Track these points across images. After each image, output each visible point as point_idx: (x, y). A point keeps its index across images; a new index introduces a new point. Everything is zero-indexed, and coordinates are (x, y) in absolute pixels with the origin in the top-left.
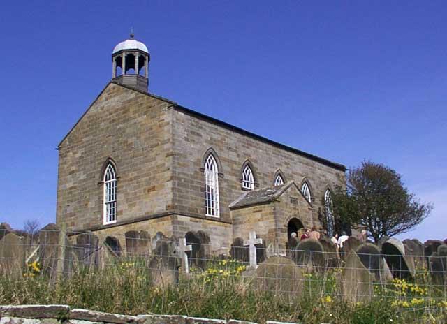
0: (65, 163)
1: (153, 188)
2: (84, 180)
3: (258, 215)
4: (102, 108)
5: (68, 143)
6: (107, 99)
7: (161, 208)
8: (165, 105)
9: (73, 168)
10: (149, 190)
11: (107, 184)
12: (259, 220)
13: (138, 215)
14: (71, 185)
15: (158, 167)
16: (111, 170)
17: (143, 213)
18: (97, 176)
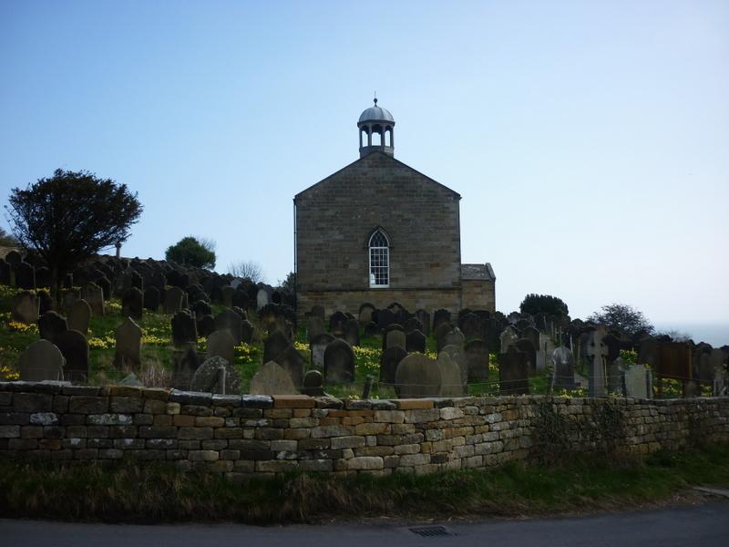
0: (309, 217)
1: (437, 265)
2: (342, 241)
3: (478, 290)
4: (365, 174)
5: (311, 196)
6: (370, 167)
7: (448, 283)
8: (450, 196)
9: (321, 225)
10: (432, 266)
11: (372, 250)
12: (479, 293)
13: (418, 285)
14: (321, 242)
15: (442, 247)
16: (379, 238)
17: (425, 284)
18: (361, 241)
